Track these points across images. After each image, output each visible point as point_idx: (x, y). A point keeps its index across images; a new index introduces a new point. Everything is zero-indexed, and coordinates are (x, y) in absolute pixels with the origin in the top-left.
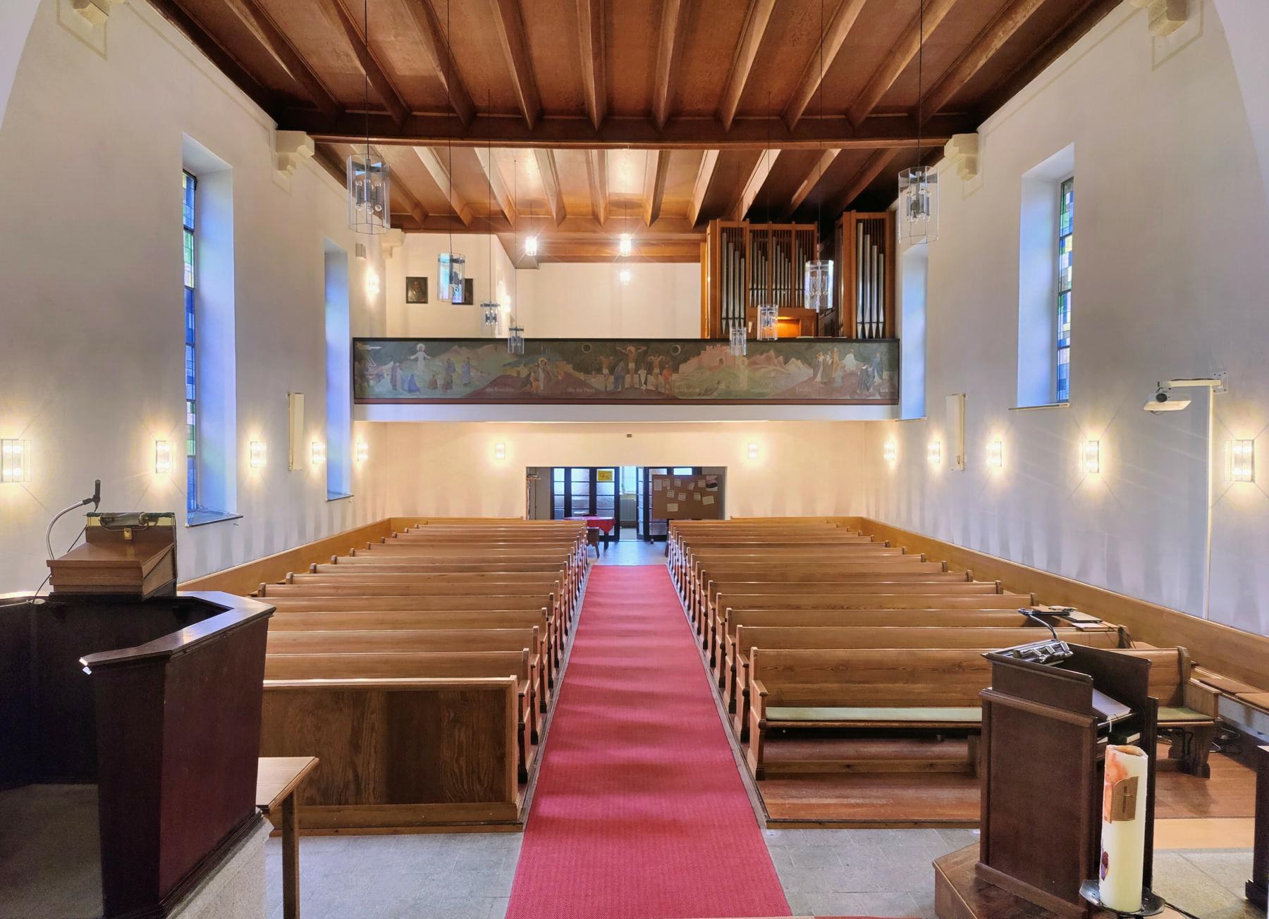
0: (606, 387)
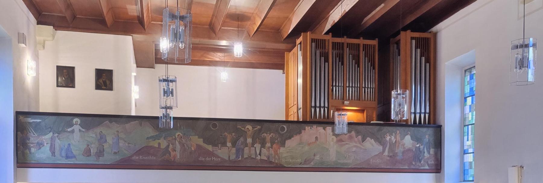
0: (229, 157)
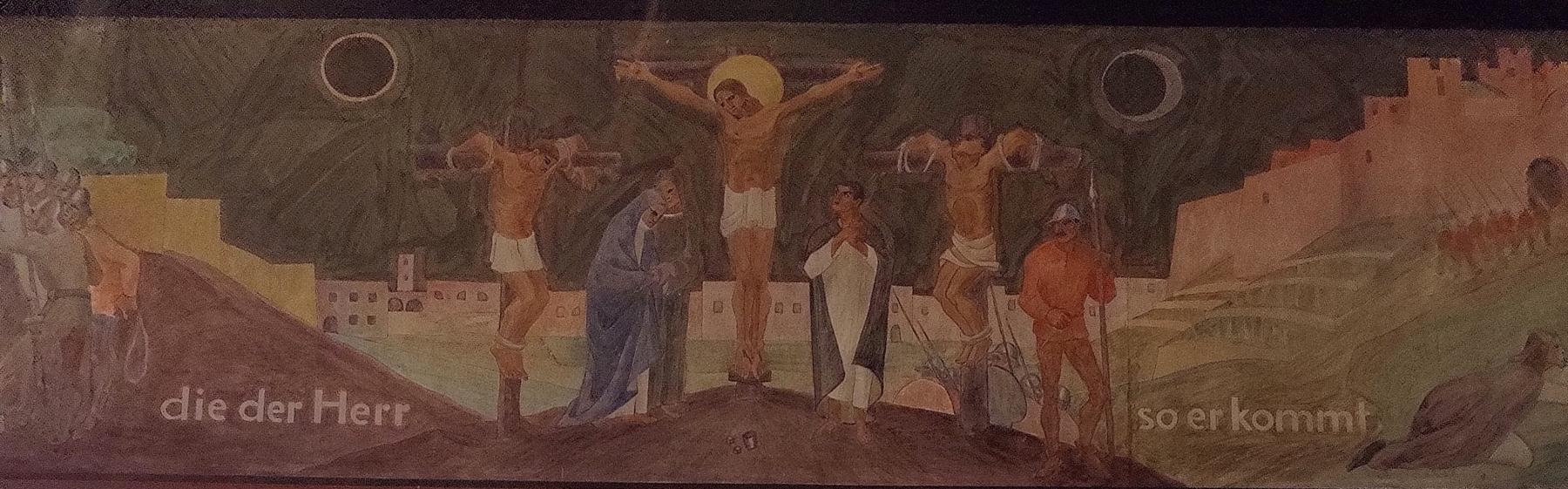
0: (512, 387)
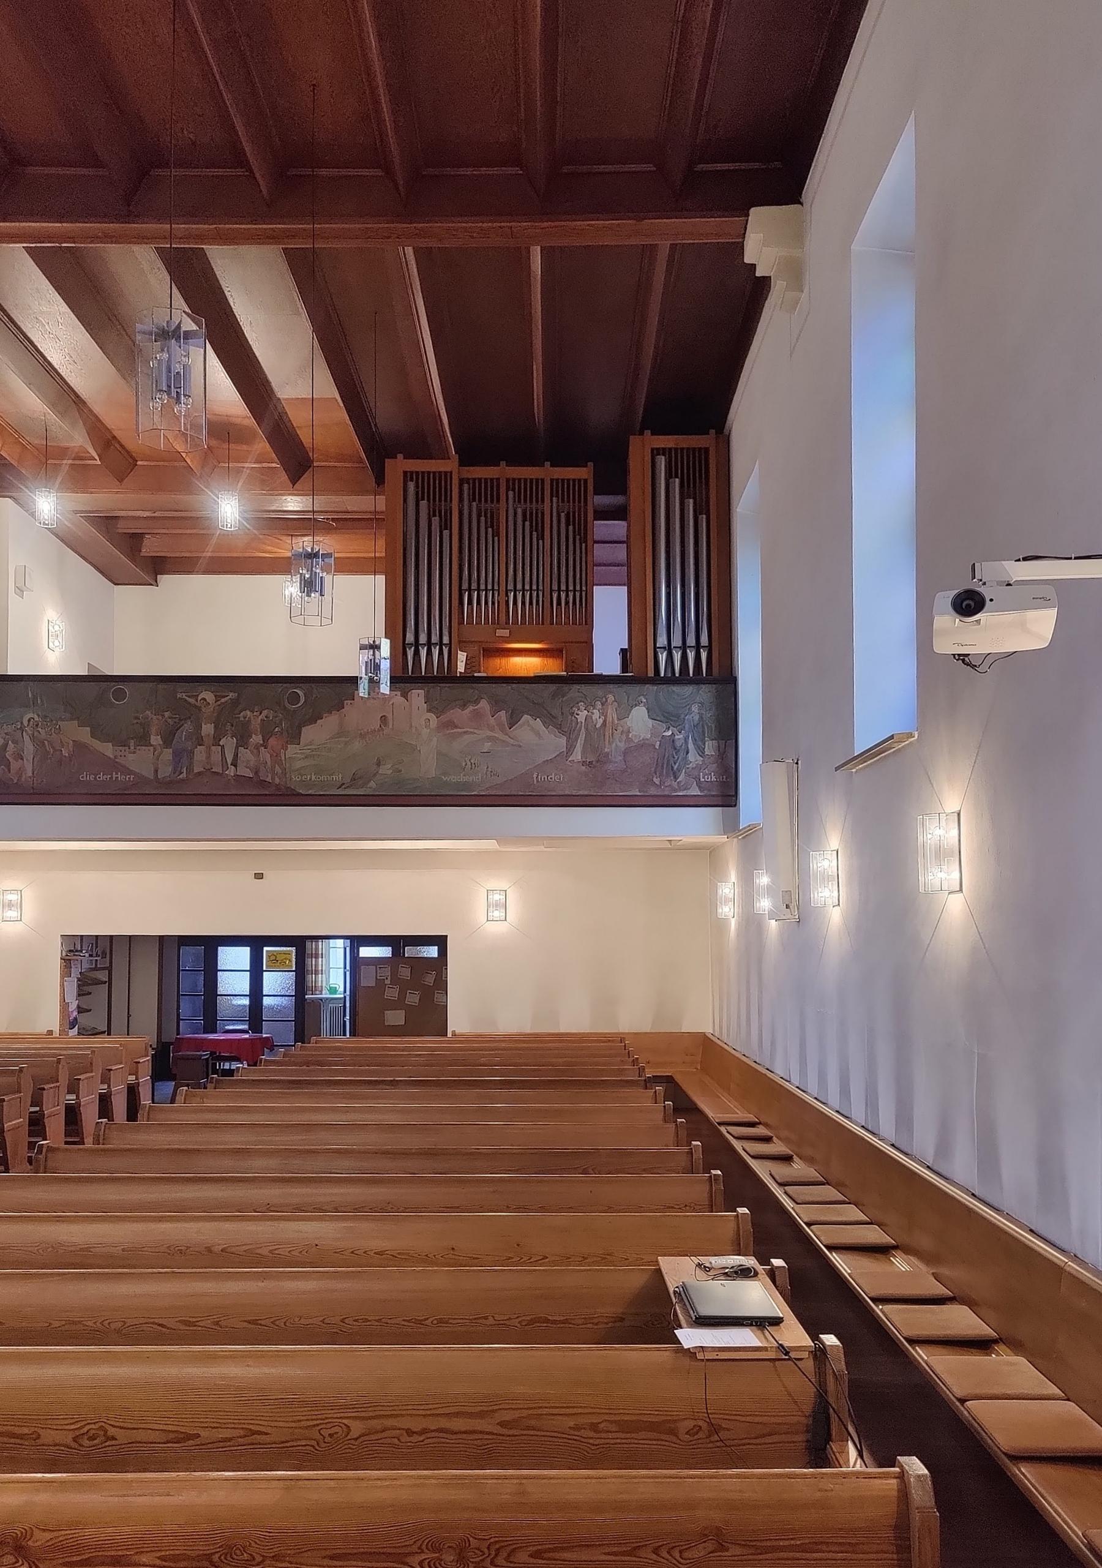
0: (156, 771)
